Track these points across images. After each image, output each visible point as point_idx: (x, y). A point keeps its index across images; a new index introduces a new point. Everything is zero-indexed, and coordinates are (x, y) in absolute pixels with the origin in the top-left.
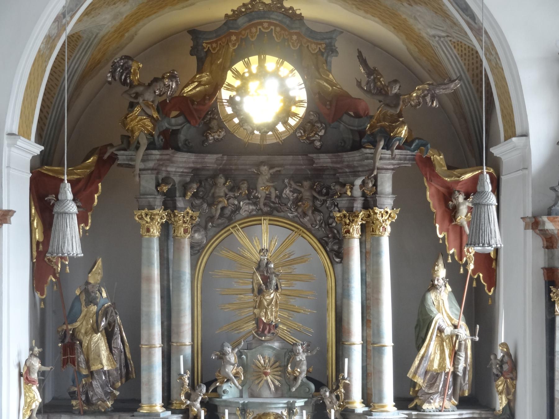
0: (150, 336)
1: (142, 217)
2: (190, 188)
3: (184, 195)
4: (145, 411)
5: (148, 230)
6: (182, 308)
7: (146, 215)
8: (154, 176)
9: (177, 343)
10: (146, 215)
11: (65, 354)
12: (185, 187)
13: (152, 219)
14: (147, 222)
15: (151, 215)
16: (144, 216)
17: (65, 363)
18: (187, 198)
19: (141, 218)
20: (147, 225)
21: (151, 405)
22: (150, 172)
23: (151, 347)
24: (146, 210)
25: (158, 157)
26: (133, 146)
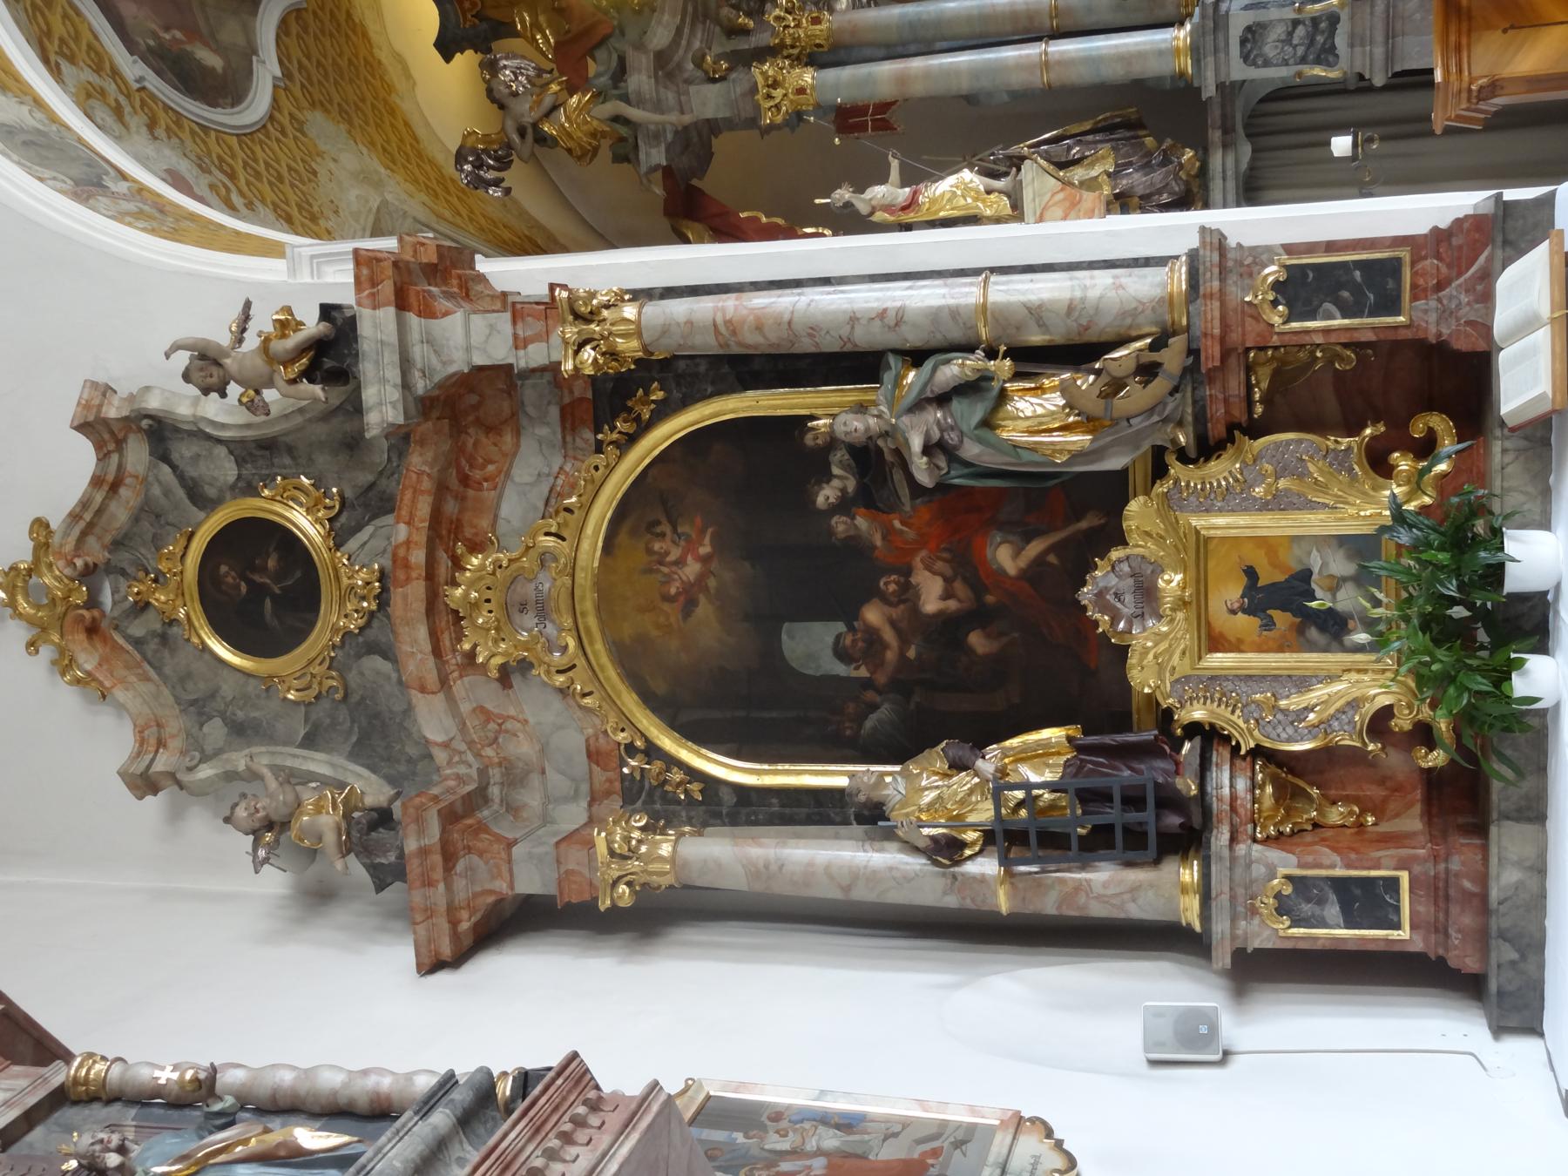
0: (1020, 66)
1: (776, 106)
2: (729, 20)
3: (744, 32)
4: (1189, 62)
5: (801, 91)
6: (975, 12)
7: (769, 97)
8: (692, 89)
9: (1051, 18)
10: (769, 97)
11: (862, 127)
12: (735, 31)
13: (775, 84)
14: (785, 95)
15: (768, 86)
16: (772, 103)
17: (884, 126)
18: (751, 23)
19: (778, 107)
20: (791, 96)
21: (1176, 52)
22: (683, 98)
23: (1046, 64)
24: (759, 97)
25: (644, 78)
26: (623, 131)
